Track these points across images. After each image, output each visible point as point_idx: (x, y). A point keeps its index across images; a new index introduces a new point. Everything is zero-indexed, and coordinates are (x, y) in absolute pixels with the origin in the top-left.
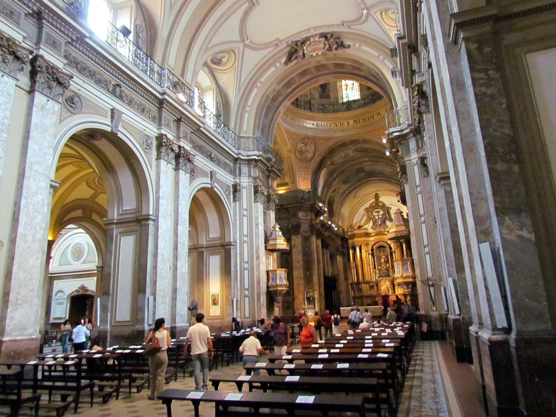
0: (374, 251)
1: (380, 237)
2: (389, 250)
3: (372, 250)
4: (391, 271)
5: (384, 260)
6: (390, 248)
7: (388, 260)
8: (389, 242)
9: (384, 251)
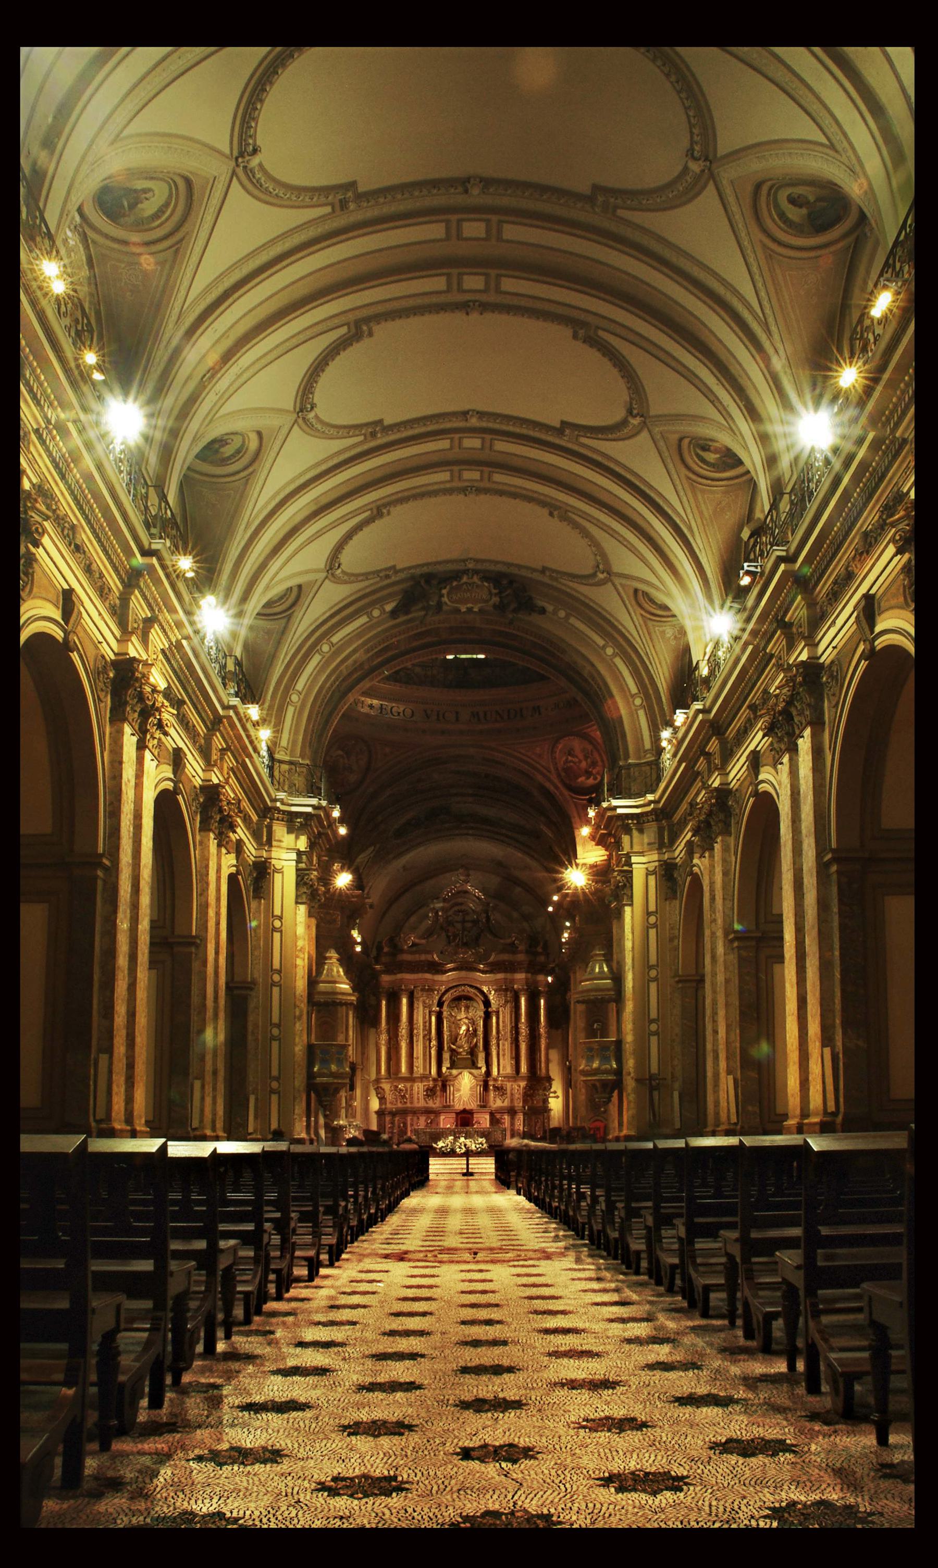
0: (445, 1007)
1: (463, 974)
2: (482, 1006)
3: (440, 1004)
4: (481, 1056)
5: (468, 1030)
6: (487, 1003)
7: (475, 1030)
8: (485, 989)
9: (467, 1008)
